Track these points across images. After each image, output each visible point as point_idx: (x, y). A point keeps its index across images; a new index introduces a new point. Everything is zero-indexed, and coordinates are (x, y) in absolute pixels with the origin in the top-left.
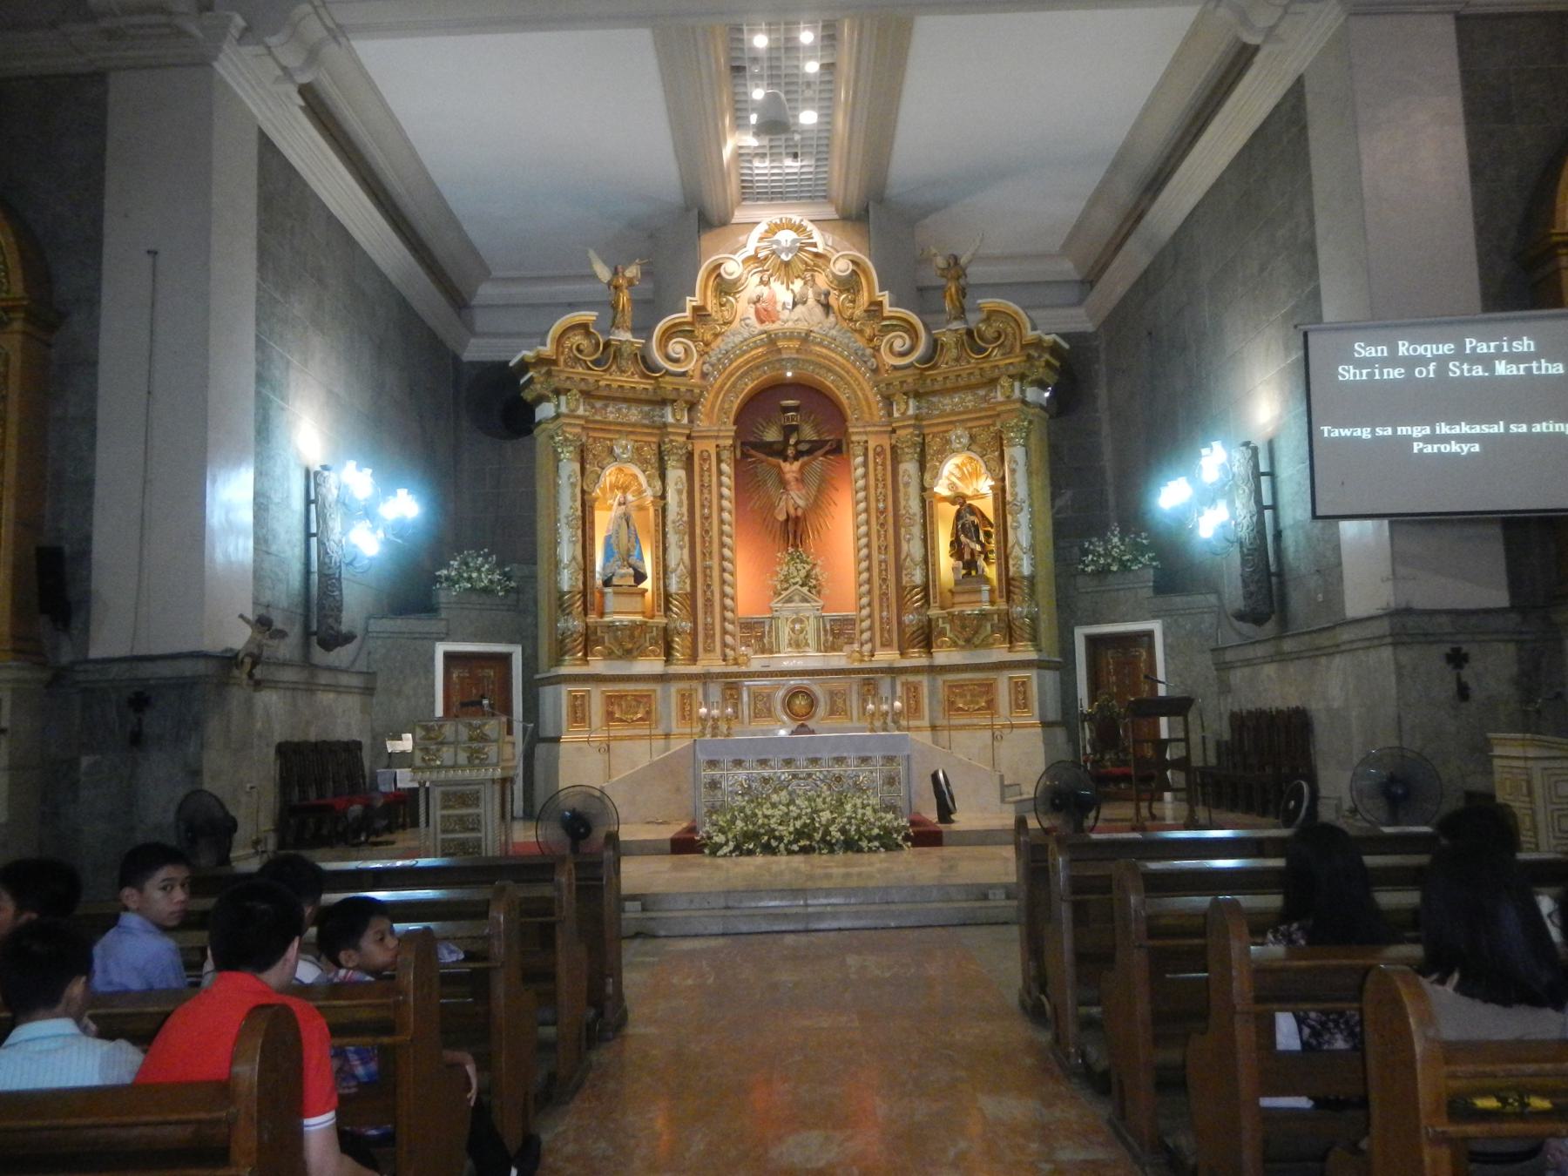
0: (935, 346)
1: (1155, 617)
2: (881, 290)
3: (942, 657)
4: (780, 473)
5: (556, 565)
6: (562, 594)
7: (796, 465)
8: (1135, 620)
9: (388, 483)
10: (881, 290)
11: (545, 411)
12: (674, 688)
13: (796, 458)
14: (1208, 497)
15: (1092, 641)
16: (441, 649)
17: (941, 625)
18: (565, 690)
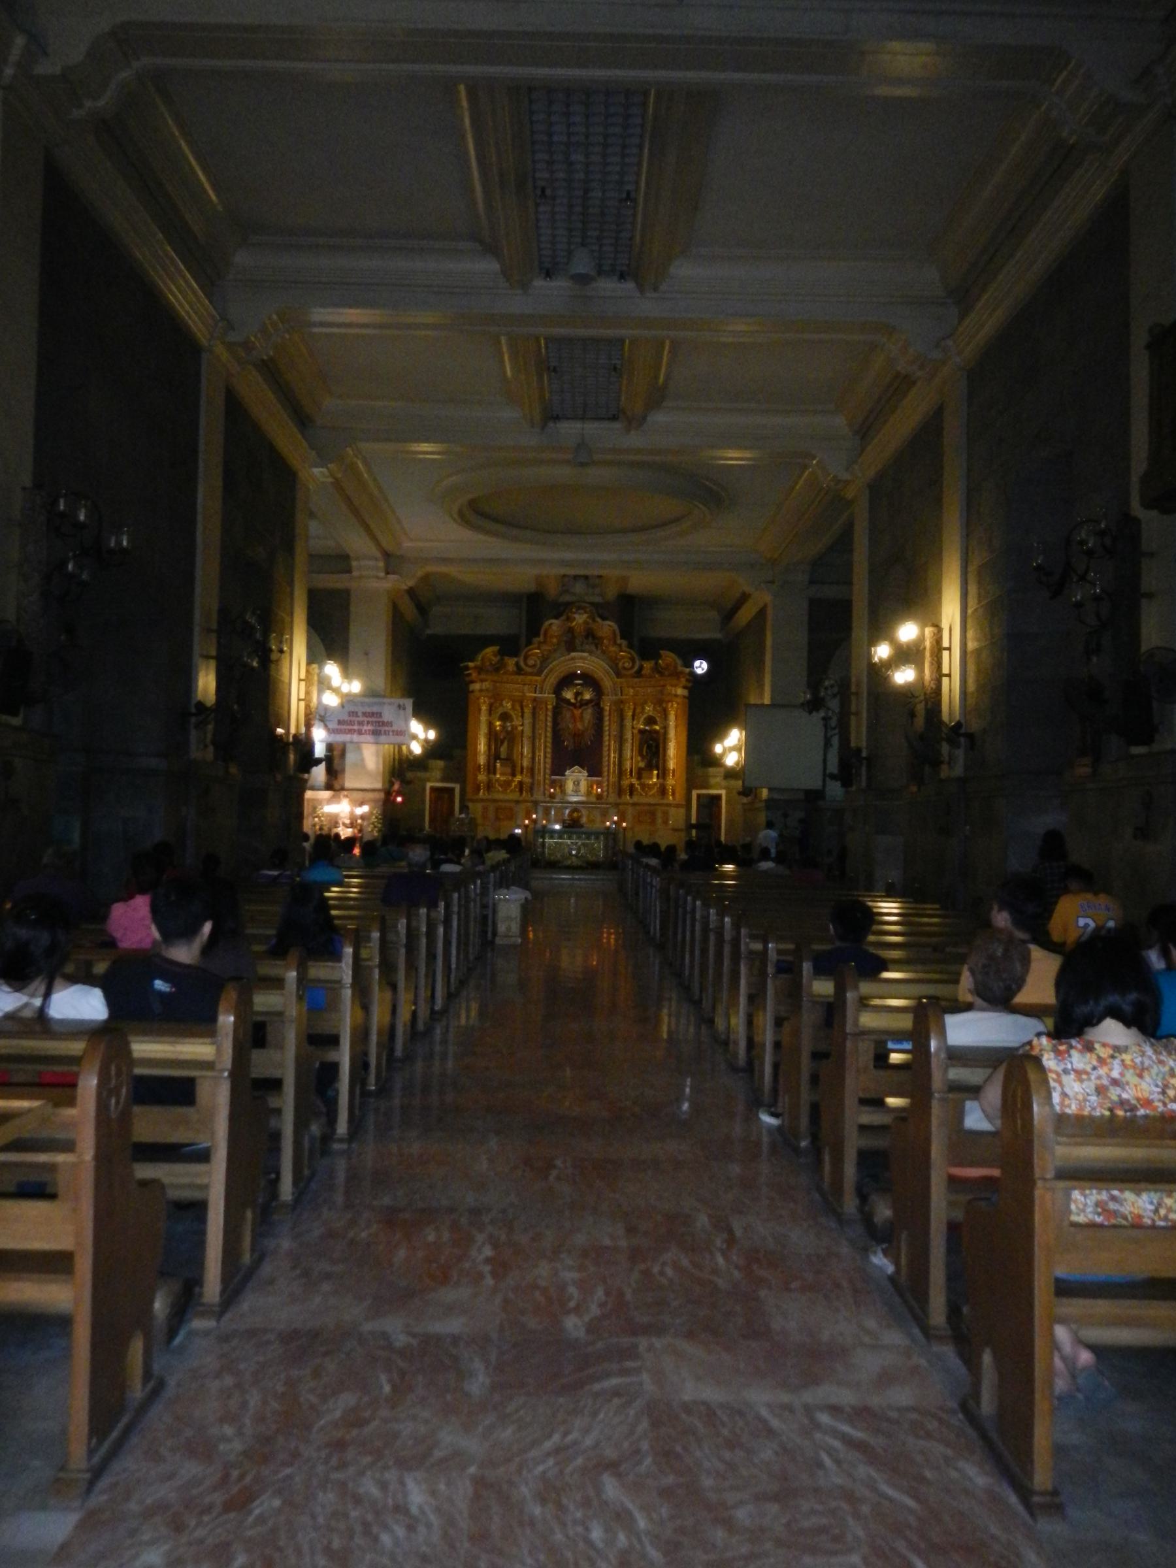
0: (641, 668)
1: (724, 788)
2: (621, 639)
3: (635, 799)
4: (573, 716)
5: (476, 753)
6: (480, 766)
7: (580, 711)
8: (717, 789)
9: (427, 728)
10: (621, 639)
11: (476, 686)
12: (523, 806)
13: (580, 707)
14: (732, 749)
15: (699, 796)
16: (429, 785)
17: (636, 786)
18: (479, 806)
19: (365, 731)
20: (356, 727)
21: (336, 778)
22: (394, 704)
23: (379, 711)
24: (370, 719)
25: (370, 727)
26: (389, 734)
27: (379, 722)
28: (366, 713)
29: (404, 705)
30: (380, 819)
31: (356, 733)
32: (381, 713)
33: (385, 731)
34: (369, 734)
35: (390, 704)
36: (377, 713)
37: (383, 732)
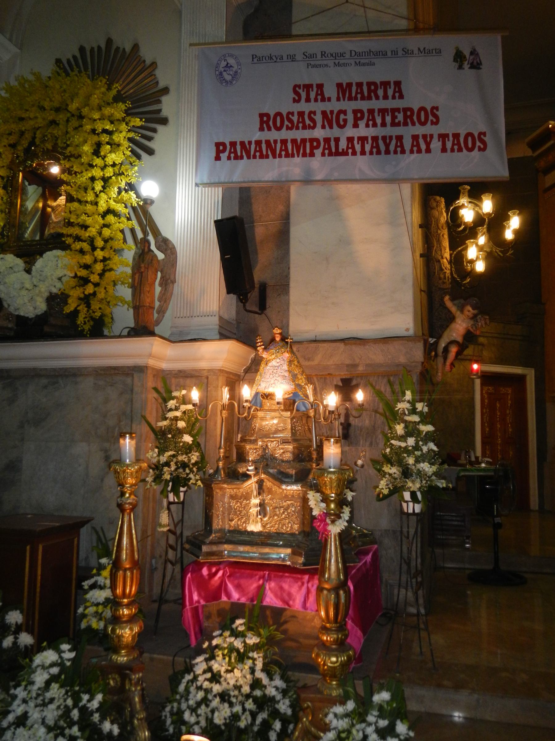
19: (350, 140)
20: (319, 133)
21: (262, 306)
22: (439, 52)
23: (392, 78)
24: (364, 105)
25: (363, 131)
26: (428, 150)
27: (394, 111)
28: (349, 85)
29: (473, 52)
30: (428, 437)
31: (318, 152)
32: (398, 84)
33: (415, 138)
34: (363, 153)
35: (425, 52)
36: (385, 85)
37: (407, 143)
